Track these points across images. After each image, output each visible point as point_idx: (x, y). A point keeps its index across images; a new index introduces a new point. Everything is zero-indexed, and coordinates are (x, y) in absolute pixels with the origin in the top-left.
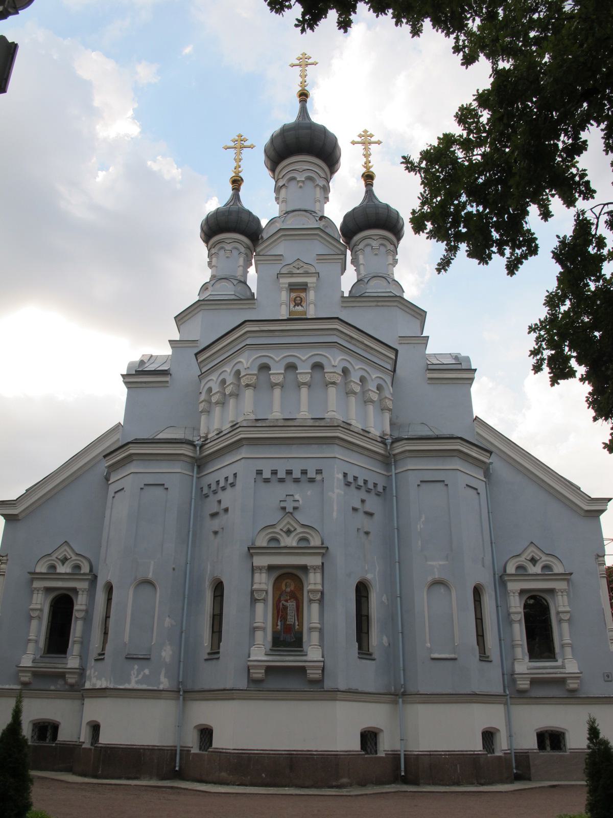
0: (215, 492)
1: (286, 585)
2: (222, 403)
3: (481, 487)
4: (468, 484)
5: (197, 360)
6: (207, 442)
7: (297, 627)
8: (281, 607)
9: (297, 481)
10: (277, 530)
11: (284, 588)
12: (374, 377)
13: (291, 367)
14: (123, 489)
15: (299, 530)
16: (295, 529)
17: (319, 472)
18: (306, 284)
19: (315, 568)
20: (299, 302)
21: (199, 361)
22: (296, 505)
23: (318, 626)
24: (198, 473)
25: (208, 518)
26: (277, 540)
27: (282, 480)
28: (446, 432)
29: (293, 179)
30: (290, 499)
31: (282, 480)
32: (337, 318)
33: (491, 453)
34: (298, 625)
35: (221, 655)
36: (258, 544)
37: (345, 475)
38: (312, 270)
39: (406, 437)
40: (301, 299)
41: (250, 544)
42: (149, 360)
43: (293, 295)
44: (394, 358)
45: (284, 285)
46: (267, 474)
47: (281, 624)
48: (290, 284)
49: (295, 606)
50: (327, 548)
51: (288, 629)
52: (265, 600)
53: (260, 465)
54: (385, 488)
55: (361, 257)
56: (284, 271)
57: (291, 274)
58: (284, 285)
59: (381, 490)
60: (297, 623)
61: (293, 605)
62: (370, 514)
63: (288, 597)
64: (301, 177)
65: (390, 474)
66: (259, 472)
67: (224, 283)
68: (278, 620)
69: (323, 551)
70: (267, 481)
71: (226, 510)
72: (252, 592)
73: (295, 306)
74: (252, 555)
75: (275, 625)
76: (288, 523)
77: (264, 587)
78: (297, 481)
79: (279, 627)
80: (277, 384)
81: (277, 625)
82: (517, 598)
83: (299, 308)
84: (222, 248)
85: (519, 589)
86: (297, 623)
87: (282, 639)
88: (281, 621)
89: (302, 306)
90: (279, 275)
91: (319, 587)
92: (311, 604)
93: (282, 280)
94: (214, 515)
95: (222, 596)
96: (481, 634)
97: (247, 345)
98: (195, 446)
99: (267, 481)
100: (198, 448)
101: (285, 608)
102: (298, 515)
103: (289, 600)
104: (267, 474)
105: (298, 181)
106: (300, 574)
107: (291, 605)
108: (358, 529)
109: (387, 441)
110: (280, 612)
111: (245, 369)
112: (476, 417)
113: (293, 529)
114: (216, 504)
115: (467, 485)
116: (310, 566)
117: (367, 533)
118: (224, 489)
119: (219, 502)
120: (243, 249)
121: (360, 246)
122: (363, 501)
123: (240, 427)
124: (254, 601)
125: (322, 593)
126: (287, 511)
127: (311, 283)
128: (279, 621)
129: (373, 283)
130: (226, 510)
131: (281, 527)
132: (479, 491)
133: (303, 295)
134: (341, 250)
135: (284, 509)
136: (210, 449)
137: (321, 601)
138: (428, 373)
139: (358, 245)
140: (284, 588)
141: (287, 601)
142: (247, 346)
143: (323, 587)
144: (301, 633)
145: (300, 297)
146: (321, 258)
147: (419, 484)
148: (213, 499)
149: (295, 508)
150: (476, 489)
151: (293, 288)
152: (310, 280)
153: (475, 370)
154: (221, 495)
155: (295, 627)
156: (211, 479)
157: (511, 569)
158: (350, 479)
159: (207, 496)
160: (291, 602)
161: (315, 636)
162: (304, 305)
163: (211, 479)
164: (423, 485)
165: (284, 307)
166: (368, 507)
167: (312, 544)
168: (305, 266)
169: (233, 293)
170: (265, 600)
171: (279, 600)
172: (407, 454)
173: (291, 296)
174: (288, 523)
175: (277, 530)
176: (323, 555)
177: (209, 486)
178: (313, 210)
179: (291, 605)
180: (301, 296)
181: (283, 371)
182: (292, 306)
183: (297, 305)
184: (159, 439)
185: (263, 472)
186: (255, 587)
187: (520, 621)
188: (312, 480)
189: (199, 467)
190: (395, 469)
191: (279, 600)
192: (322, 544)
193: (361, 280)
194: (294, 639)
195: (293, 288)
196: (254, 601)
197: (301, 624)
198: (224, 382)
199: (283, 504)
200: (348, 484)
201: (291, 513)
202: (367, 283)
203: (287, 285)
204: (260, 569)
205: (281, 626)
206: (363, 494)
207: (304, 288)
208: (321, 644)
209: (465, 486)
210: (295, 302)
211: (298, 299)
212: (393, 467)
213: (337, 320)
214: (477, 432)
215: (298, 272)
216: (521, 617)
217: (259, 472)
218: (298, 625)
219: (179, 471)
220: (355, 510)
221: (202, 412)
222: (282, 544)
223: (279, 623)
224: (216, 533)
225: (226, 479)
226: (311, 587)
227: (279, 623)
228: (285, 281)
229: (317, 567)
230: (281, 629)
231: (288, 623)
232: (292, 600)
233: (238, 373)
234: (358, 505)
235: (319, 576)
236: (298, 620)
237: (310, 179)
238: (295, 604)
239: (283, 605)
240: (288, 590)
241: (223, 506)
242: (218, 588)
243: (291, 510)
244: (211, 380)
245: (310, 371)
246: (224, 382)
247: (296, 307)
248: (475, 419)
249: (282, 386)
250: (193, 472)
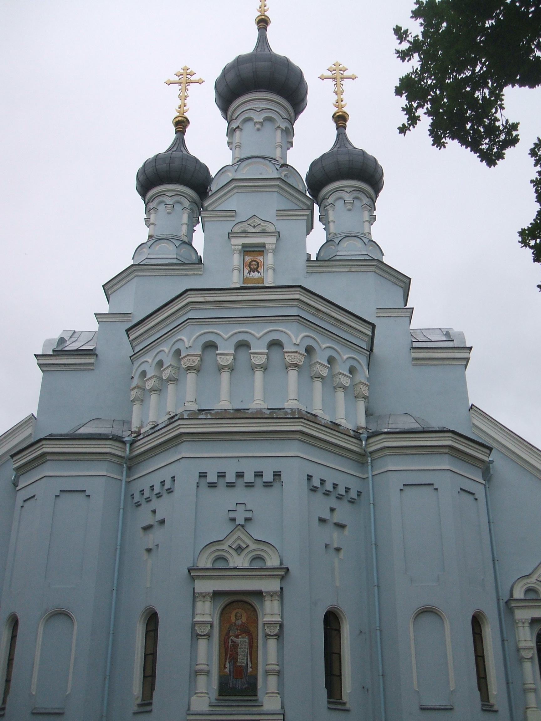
0: (148, 500)
1: (236, 616)
2: (159, 390)
3: (479, 491)
4: (462, 488)
5: (129, 338)
6: (139, 438)
7: (250, 670)
8: (230, 644)
9: (249, 485)
10: (225, 547)
11: (233, 619)
12: (345, 357)
13: (243, 345)
14: (34, 496)
15: (253, 546)
16: (248, 546)
17: (277, 475)
18: (263, 245)
19: (272, 595)
20: (255, 267)
21: (131, 338)
22: (249, 515)
23: (277, 668)
24: (128, 476)
25: (141, 533)
26: (225, 560)
27: (231, 485)
28: (435, 424)
29: (249, 119)
30: (241, 508)
31: (231, 485)
32: (300, 286)
33: (490, 449)
34: (251, 667)
35: (154, 707)
36: (201, 565)
37: (310, 477)
38: (271, 228)
39: (386, 430)
40: (258, 263)
41: (190, 565)
42: (71, 337)
43: (248, 259)
44: (371, 334)
45: (237, 247)
46: (212, 478)
47: (230, 666)
48: (244, 246)
49: (247, 644)
50: (288, 569)
51: (239, 672)
52: (209, 636)
53: (203, 466)
54: (359, 494)
55: (331, 213)
56: (236, 230)
57: (245, 233)
58: (237, 247)
59: (355, 496)
60: (250, 665)
61: (245, 641)
62: (341, 526)
63: (239, 631)
64: (258, 118)
65: (364, 476)
66: (203, 475)
67: (164, 245)
68: (225, 661)
69: (282, 573)
70: (212, 485)
71: (162, 522)
72: (194, 625)
73: (249, 272)
74: (193, 579)
75: (222, 667)
76: (239, 538)
77: (208, 619)
78: (249, 485)
79: (227, 670)
80: (225, 367)
81: (225, 668)
82: (527, 629)
83: (255, 275)
84: (162, 202)
85: (530, 618)
86: (250, 665)
87: (231, 685)
88: (229, 662)
89: (258, 272)
90: (231, 235)
91: (278, 619)
92: (267, 640)
93: (234, 241)
94: (147, 528)
95: (156, 630)
96: (339, 674)
97: (189, 319)
98: (124, 443)
99: (212, 485)
100: (128, 445)
102: (252, 529)
103: (240, 635)
104: (212, 478)
105: (255, 123)
106: (255, 602)
107: (243, 641)
108: (327, 546)
109: (362, 436)
111: (187, 348)
112: (472, 405)
113: (244, 546)
114: (150, 514)
115: (461, 489)
116: (266, 593)
117: (338, 550)
118: (159, 496)
119: (154, 512)
120: (187, 204)
121: (330, 200)
122: (332, 510)
123: (179, 419)
124: (196, 636)
125: (281, 626)
126: (237, 523)
127: (270, 244)
128: (227, 663)
129: (345, 244)
130: (162, 522)
131: (229, 543)
132: (477, 496)
133: (260, 258)
134: (306, 204)
135: (233, 520)
136: (142, 447)
137: (279, 636)
138: (413, 352)
139: (328, 199)
140: (233, 619)
141: (237, 637)
142: (189, 321)
143: (282, 618)
144: (255, 677)
145: (256, 261)
146: (282, 213)
147: (402, 488)
148: (146, 509)
149: (247, 520)
150: (473, 494)
151: (247, 250)
152: (270, 241)
153: (471, 348)
154: (155, 504)
155: (247, 669)
156: (145, 484)
157: (519, 594)
158: (316, 483)
159: (138, 505)
160: (243, 638)
161: (273, 680)
162: (261, 270)
163: (145, 484)
164: (407, 489)
165: (236, 273)
166: (337, 518)
167: (269, 564)
168: (262, 223)
169: (175, 256)
170: (209, 636)
171: (228, 636)
172: (388, 452)
173: (246, 260)
174: (239, 538)
175: (225, 547)
176: (282, 578)
177: (142, 492)
178: (273, 157)
179: (243, 641)
180: (257, 260)
181: (233, 352)
182: (246, 271)
183: (252, 270)
184: (80, 435)
185: (208, 475)
186: (198, 619)
187: (532, 659)
188: (268, 485)
189: (129, 468)
190: (372, 472)
191: (228, 636)
192: (281, 564)
193: (331, 240)
194: (247, 685)
195: (247, 250)
196: (196, 636)
197: (255, 666)
198: (160, 364)
199: (232, 515)
200: (314, 489)
201: (243, 526)
202: (338, 244)
203: (240, 247)
204: (204, 596)
205: (230, 670)
206: (332, 502)
207: (260, 249)
208: (280, 692)
209: (459, 490)
210: (250, 267)
211: (254, 263)
212: (370, 467)
213: (299, 289)
214: (473, 424)
215: (254, 230)
216: (533, 653)
217: (203, 475)
218: (251, 667)
219: (104, 473)
220: (322, 521)
221: (133, 401)
222: (231, 565)
223: (228, 665)
224: (149, 550)
225: (163, 483)
226: (268, 619)
227: (228, 665)
228: (238, 242)
229: (275, 593)
230: (230, 672)
231: (238, 665)
232: (244, 635)
233: (178, 352)
234: (326, 515)
235: (276, 604)
236: (251, 661)
237: (269, 119)
238: (247, 640)
239: (232, 641)
240: (239, 622)
241: (159, 517)
243: (243, 523)
244: (146, 361)
245: (267, 351)
246: (160, 364)
247: (252, 273)
248: (471, 408)
249: (231, 368)
250: (122, 476)
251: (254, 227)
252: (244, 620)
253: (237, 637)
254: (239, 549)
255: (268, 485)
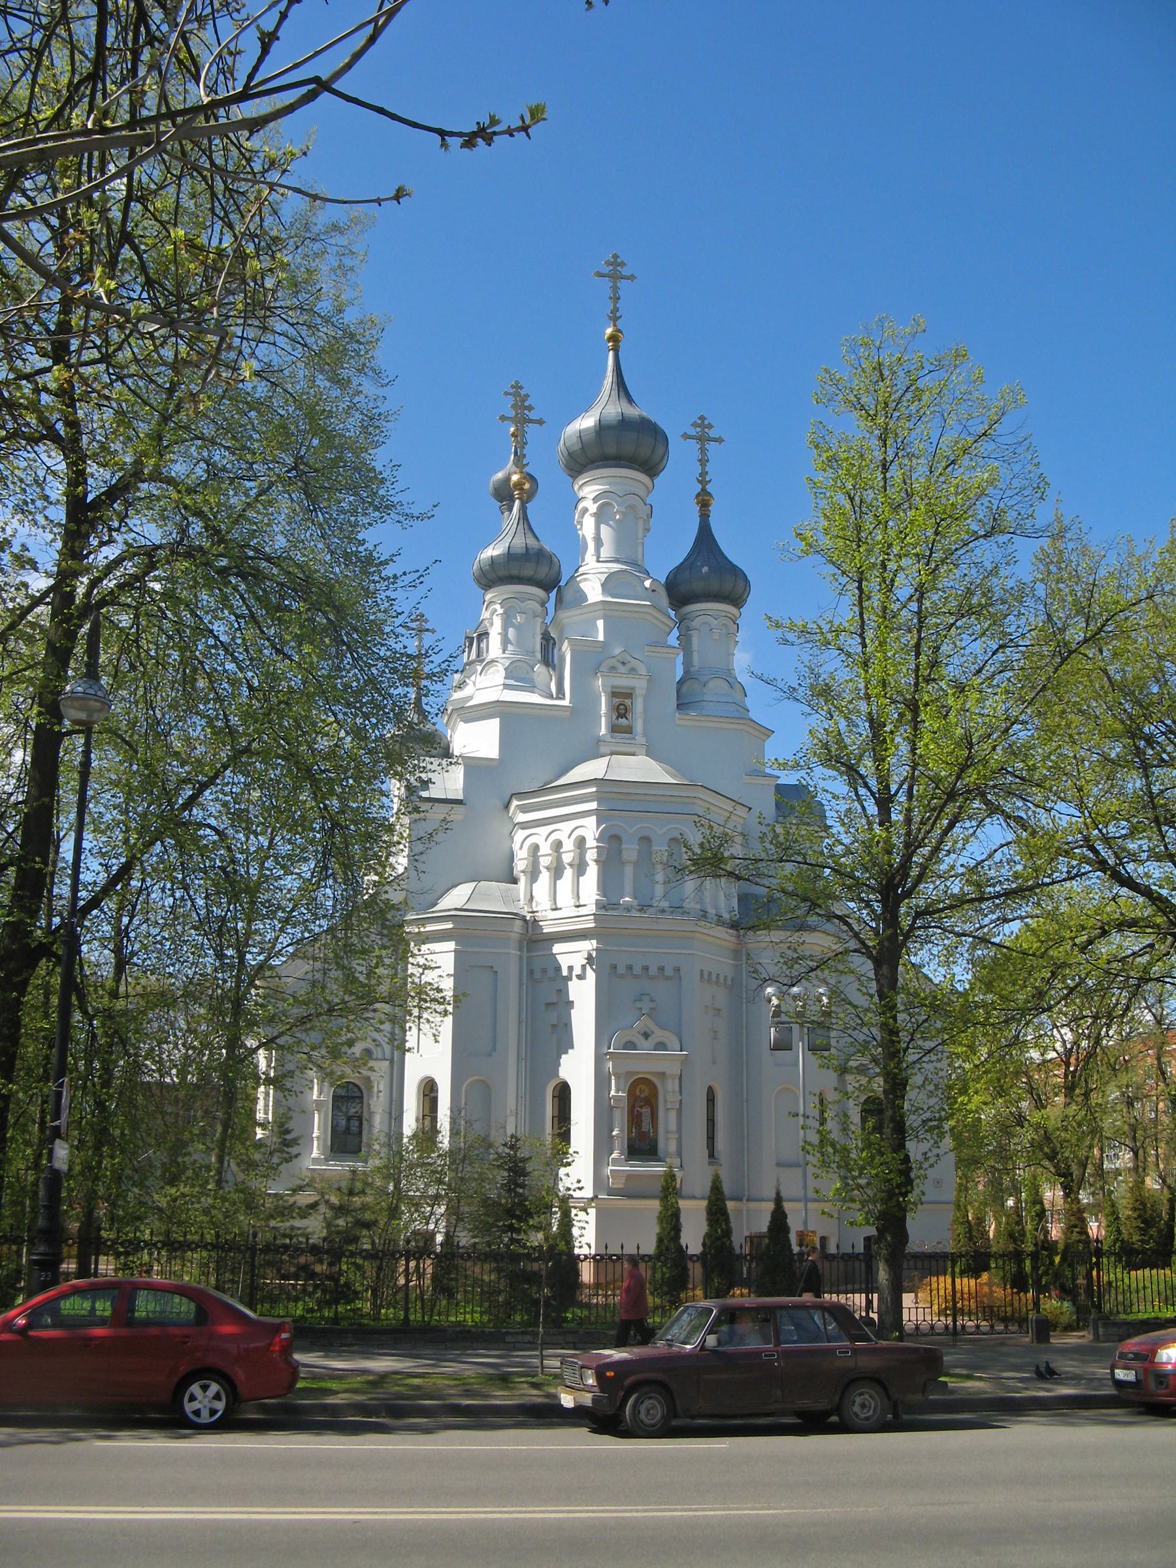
11: (638, 1093)
17: (677, 970)
18: (633, 689)
27: (636, 977)
31: (636, 977)
43: (617, 701)
51: (642, 1135)
54: (733, 979)
70: (622, 976)
75: (630, 1132)
78: (653, 978)
83: (623, 721)
101: (640, 1114)
104: (621, 970)
107: (646, 1111)
110: (634, 1119)
133: (628, 702)
179: (646, 1111)
183: (620, 716)
188: (669, 978)
197: (656, 1132)
224: (554, 1026)
240: (643, 1096)
242: (563, 1093)
251: (623, 663)
252: (646, 1093)
253: (641, 1107)
254: (646, 1035)
255: (669, 978)
